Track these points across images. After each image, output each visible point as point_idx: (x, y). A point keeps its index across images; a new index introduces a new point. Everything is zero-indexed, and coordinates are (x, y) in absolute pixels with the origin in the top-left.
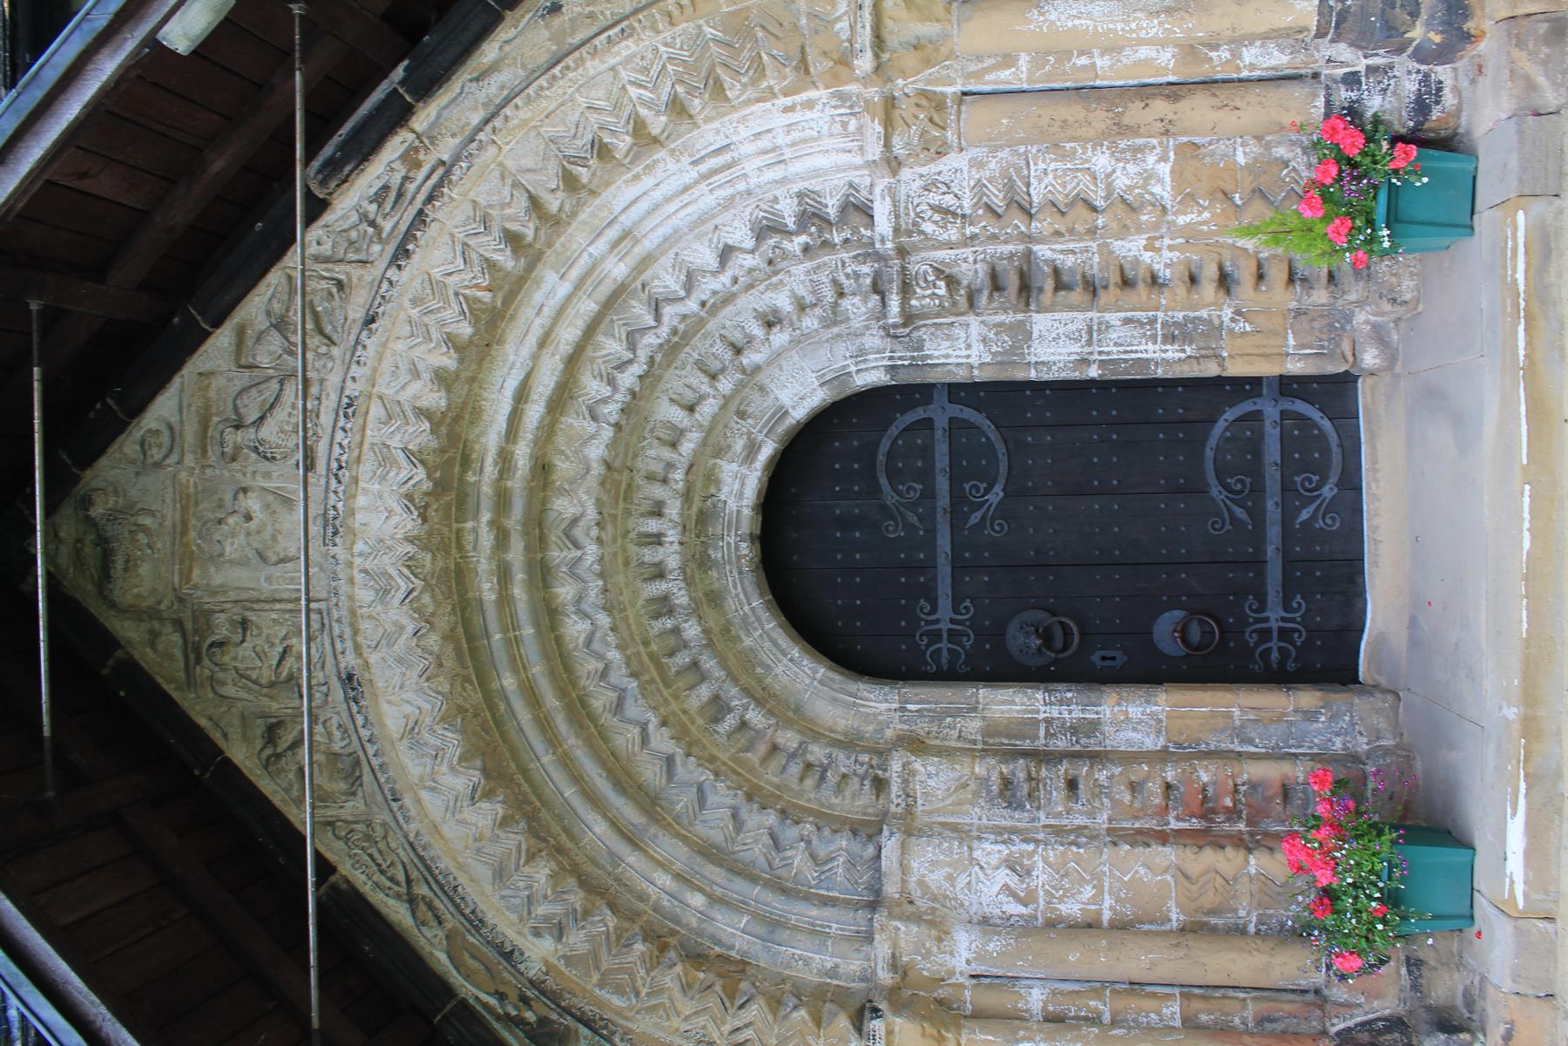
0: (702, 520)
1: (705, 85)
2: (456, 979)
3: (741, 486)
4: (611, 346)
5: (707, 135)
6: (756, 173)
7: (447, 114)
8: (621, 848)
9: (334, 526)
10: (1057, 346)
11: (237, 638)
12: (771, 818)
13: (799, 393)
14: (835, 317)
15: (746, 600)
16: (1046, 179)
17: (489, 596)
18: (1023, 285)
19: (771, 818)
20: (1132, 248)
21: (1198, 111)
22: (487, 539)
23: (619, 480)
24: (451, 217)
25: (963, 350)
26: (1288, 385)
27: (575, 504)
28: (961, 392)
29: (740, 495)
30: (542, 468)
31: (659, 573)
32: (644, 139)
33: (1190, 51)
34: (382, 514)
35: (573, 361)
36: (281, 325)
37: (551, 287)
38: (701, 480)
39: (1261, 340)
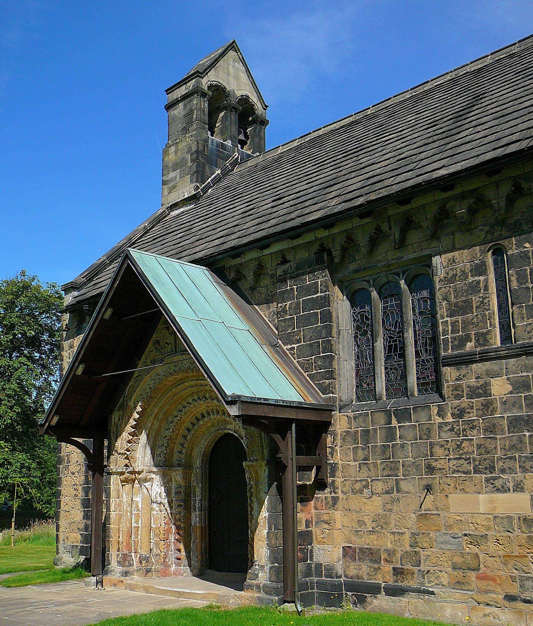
2: (128, 387)
8: (153, 416)
11: (170, 332)
12: (165, 445)
17: (186, 384)
19: (165, 445)
22: (193, 383)
29: (229, 429)
31: (209, 414)
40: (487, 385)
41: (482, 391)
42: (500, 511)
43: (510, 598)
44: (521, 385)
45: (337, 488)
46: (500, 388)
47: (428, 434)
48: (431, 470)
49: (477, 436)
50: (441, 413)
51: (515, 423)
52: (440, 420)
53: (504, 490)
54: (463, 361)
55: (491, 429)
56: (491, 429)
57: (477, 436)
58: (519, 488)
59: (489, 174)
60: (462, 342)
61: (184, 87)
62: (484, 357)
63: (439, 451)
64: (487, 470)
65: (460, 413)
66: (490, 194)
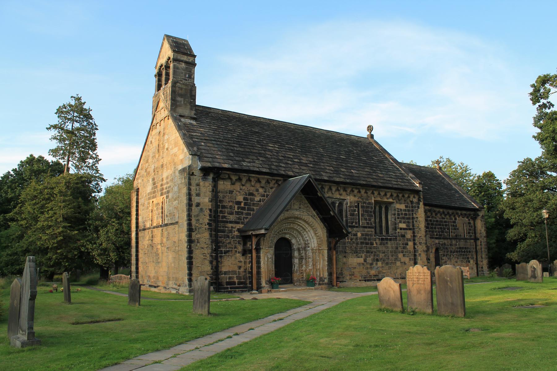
0: (285, 233)
1: (318, 238)
3: (287, 236)
4: (301, 229)
5: (315, 237)
6: (312, 240)
7: (318, 220)
9: (296, 210)
10: (296, 261)
13: (293, 241)
14: (299, 245)
15: (280, 236)
16: (310, 260)
18: (301, 259)
20: (304, 266)
21: (315, 270)
23: (293, 228)
24: (313, 220)
25: (296, 254)
26: (292, 279)
27: (292, 226)
28: (291, 253)
30: (294, 223)
32: (316, 234)
33: (319, 269)
34: (297, 213)
35: (301, 226)
36: (308, 207)
37: (307, 226)
38: (288, 233)
39: (296, 276)
40: (357, 234)
41: (356, 235)
42: (358, 262)
43: (360, 280)
44: (362, 235)
45: (309, 258)
46: (359, 235)
47: (345, 244)
48: (345, 252)
49: (355, 245)
50: (348, 239)
51: (362, 243)
52: (347, 240)
53: (359, 257)
54: (353, 227)
55: (357, 244)
56: (357, 244)
57: (355, 245)
58: (361, 257)
59: (362, 186)
60: (352, 223)
61: (186, 57)
62: (357, 227)
63: (347, 248)
64: (356, 253)
65: (352, 240)
66: (361, 190)
